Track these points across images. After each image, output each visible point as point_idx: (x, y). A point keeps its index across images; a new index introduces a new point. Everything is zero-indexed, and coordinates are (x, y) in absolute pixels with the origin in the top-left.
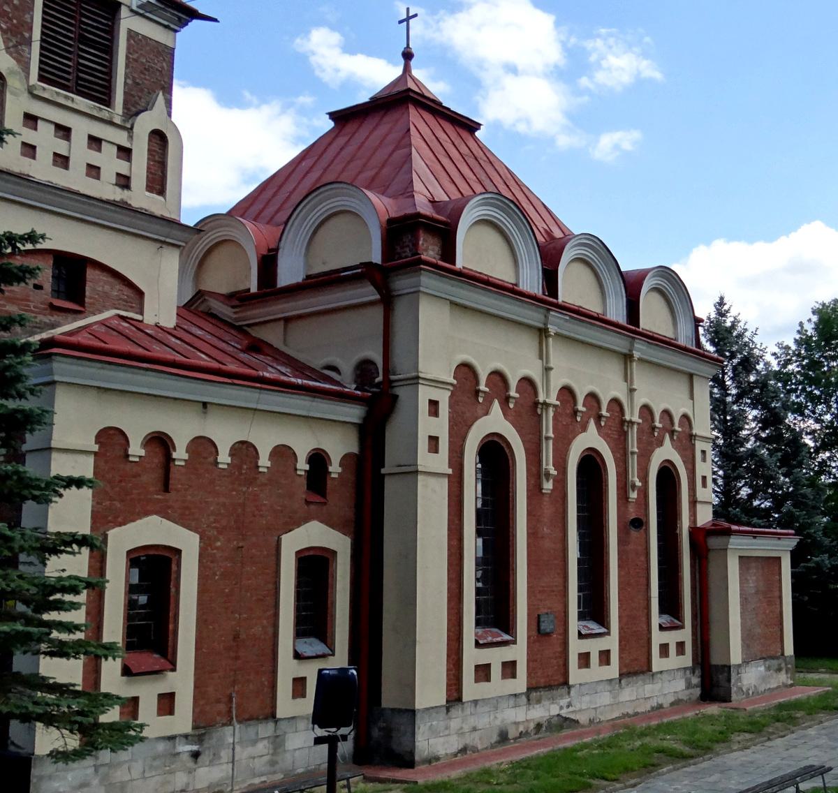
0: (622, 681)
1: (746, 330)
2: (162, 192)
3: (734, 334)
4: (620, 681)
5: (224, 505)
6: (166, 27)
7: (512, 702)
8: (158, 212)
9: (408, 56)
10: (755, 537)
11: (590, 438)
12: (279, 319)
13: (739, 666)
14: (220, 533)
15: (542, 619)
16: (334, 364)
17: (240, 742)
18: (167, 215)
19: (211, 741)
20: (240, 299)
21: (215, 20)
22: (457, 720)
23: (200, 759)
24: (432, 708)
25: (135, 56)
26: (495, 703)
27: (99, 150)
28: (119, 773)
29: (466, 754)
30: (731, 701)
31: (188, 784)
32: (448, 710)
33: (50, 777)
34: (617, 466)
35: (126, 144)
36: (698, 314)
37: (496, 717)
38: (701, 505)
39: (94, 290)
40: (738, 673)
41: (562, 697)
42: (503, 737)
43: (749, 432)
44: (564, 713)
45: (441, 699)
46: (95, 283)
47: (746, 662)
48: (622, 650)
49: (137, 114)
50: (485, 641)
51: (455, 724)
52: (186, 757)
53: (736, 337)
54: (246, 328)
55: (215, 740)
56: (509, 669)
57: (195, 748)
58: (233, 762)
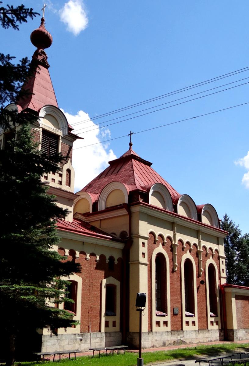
0: (199, 331)
1: (234, 225)
2: (69, 185)
3: (231, 226)
4: (198, 331)
5: (88, 270)
7: (167, 333)
8: (68, 191)
9: (131, 145)
10: (240, 289)
11: (187, 255)
12: (98, 220)
13: (236, 330)
15: (175, 309)
16: (115, 233)
18: (71, 191)
20: (87, 215)
21: (83, 139)
22: (151, 337)
26: (162, 333)
27: (55, 175)
28: (62, 342)
29: (154, 347)
30: (234, 341)
31: (79, 348)
34: (196, 264)
36: (220, 219)
37: (162, 338)
38: (222, 280)
40: (236, 332)
42: (164, 344)
43: (237, 258)
44: (182, 339)
45: (147, 331)
47: (238, 329)
48: (199, 322)
49: (64, 165)
50: (159, 314)
51: (151, 338)
52: (79, 340)
53: (231, 227)
54: (89, 223)
57: (81, 338)
58: (90, 343)
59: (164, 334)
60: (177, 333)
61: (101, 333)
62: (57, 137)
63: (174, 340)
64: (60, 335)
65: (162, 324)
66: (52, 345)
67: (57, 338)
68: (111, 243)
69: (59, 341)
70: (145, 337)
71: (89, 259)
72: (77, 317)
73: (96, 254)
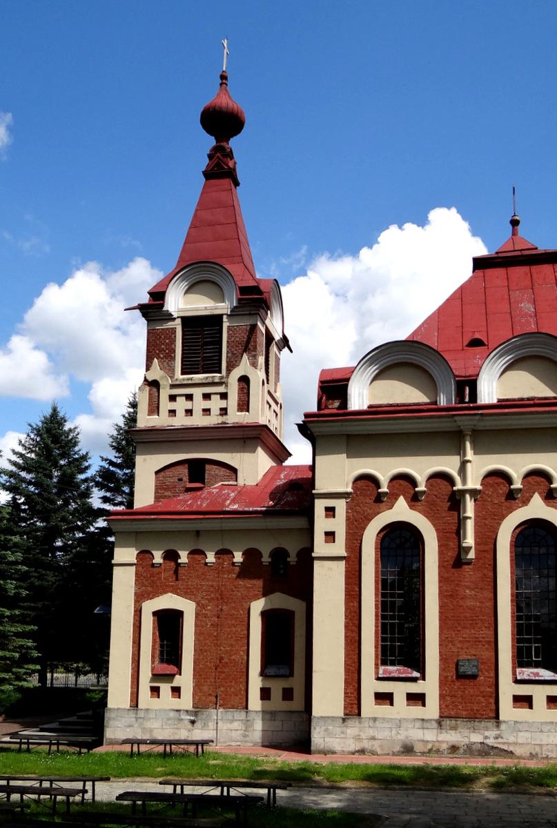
5: (212, 586)
6: (250, 314)
7: (418, 724)
14: (209, 602)
17: (222, 720)
19: (200, 716)
22: (353, 728)
23: (195, 725)
24: (328, 717)
25: (233, 339)
26: (399, 723)
32: (344, 720)
33: (114, 719)
35: (224, 391)
39: (209, 474)
41: (487, 729)
44: (491, 742)
45: (340, 712)
46: (210, 470)
55: (205, 716)
56: (417, 699)
57: (193, 718)
58: (217, 730)
59: (404, 725)
60: (469, 725)
61: (247, 712)
62: (216, 320)
63: (450, 744)
64: (141, 710)
65: (400, 699)
66: (125, 726)
67: (137, 714)
68: (267, 520)
69: (142, 720)
70: (330, 728)
71: (214, 563)
72: (186, 679)
73: (232, 550)
